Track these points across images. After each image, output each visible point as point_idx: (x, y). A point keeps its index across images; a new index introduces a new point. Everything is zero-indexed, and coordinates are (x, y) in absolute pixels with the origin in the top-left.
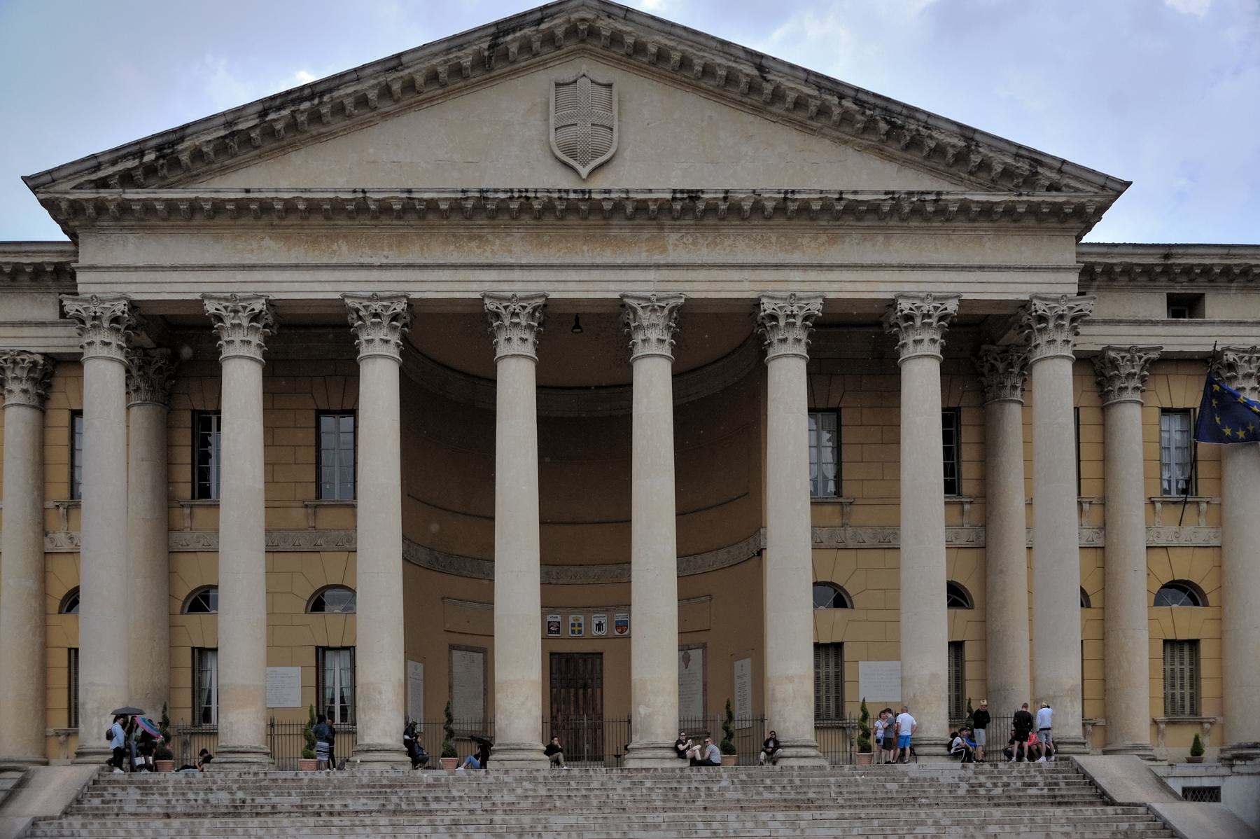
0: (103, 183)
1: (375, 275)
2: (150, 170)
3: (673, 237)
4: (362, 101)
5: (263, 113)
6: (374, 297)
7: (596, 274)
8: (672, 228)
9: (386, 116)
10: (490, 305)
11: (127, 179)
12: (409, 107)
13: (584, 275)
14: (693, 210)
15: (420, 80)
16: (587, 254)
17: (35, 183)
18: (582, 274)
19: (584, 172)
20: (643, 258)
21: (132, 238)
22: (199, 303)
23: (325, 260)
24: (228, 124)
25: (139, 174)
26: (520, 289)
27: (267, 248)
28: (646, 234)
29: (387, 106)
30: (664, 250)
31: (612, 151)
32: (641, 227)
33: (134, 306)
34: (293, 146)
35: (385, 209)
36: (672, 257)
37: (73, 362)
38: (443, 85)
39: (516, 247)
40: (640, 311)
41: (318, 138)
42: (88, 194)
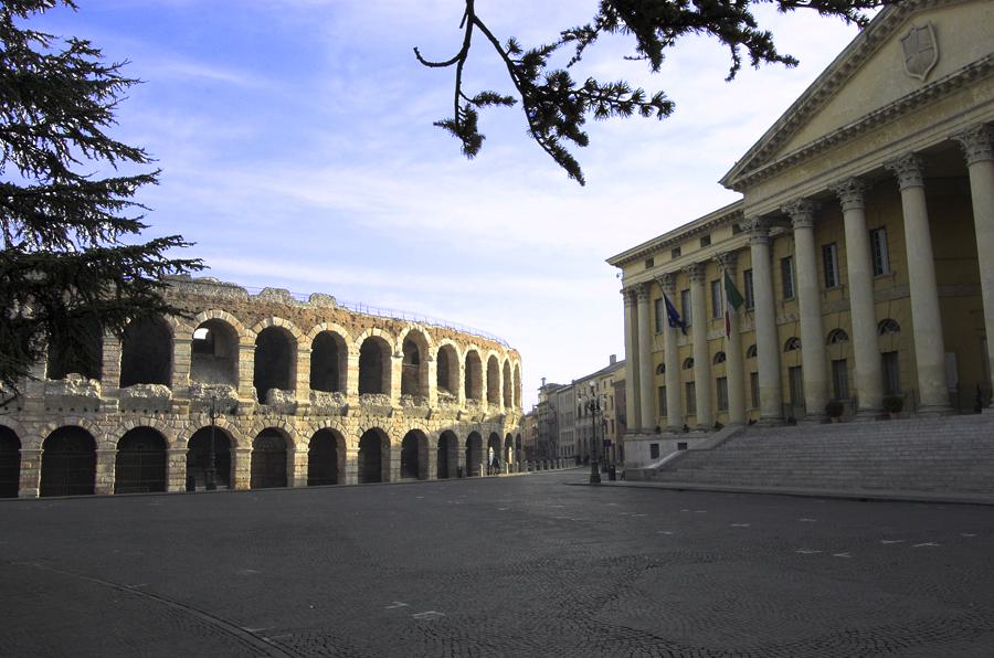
0: (743, 173)
1: (842, 170)
2: (756, 160)
3: (975, 91)
4: (822, 93)
5: (787, 118)
6: (839, 182)
7: (937, 130)
8: (974, 86)
9: (837, 93)
10: (888, 168)
11: (750, 167)
12: (845, 84)
13: (932, 132)
14: (976, 73)
15: (842, 71)
16: (931, 120)
17: (725, 182)
18: (929, 133)
19: (923, 78)
20: (961, 109)
21: (759, 189)
22: (780, 210)
23: (823, 171)
24: (776, 129)
25: (754, 164)
26: (901, 153)
27: (803, 174)
28: (961, 96)
29: (835, 89)
30: (972, 100)
31: (935, 59)
32: (956, 93)
33: (765, 217)
34: (805, 124)
35: (836, 139)
36: (977, 101)
37: (747, 249)
38: (855, 67)
39: (898, 131)
40: (963, 141)
41: (813, 116)
42: (737, 180)
